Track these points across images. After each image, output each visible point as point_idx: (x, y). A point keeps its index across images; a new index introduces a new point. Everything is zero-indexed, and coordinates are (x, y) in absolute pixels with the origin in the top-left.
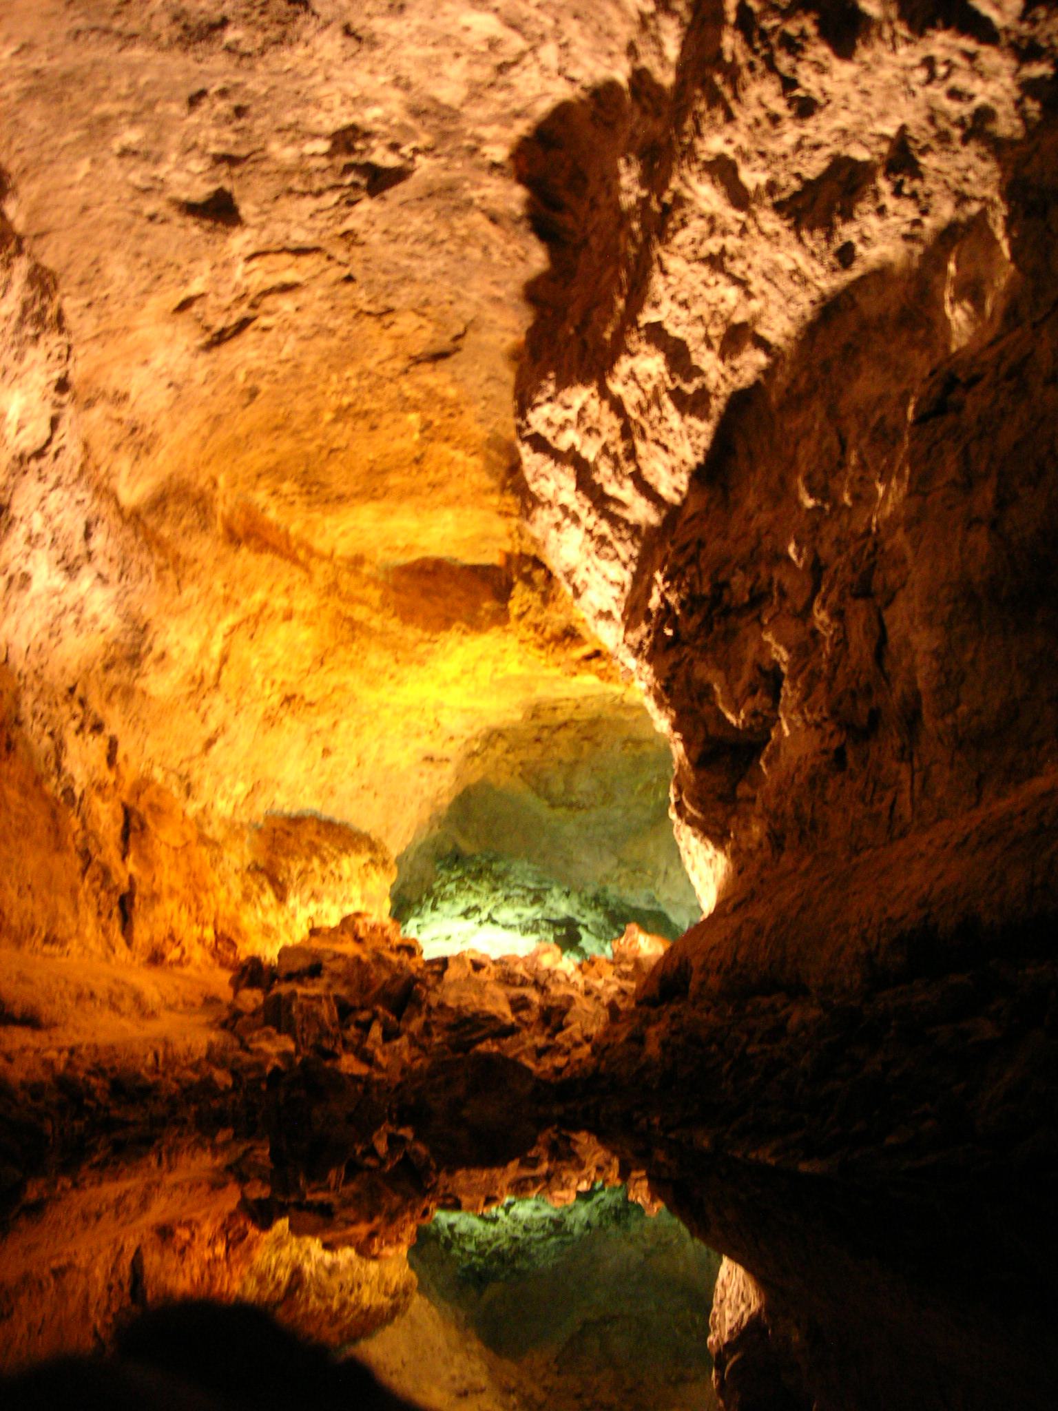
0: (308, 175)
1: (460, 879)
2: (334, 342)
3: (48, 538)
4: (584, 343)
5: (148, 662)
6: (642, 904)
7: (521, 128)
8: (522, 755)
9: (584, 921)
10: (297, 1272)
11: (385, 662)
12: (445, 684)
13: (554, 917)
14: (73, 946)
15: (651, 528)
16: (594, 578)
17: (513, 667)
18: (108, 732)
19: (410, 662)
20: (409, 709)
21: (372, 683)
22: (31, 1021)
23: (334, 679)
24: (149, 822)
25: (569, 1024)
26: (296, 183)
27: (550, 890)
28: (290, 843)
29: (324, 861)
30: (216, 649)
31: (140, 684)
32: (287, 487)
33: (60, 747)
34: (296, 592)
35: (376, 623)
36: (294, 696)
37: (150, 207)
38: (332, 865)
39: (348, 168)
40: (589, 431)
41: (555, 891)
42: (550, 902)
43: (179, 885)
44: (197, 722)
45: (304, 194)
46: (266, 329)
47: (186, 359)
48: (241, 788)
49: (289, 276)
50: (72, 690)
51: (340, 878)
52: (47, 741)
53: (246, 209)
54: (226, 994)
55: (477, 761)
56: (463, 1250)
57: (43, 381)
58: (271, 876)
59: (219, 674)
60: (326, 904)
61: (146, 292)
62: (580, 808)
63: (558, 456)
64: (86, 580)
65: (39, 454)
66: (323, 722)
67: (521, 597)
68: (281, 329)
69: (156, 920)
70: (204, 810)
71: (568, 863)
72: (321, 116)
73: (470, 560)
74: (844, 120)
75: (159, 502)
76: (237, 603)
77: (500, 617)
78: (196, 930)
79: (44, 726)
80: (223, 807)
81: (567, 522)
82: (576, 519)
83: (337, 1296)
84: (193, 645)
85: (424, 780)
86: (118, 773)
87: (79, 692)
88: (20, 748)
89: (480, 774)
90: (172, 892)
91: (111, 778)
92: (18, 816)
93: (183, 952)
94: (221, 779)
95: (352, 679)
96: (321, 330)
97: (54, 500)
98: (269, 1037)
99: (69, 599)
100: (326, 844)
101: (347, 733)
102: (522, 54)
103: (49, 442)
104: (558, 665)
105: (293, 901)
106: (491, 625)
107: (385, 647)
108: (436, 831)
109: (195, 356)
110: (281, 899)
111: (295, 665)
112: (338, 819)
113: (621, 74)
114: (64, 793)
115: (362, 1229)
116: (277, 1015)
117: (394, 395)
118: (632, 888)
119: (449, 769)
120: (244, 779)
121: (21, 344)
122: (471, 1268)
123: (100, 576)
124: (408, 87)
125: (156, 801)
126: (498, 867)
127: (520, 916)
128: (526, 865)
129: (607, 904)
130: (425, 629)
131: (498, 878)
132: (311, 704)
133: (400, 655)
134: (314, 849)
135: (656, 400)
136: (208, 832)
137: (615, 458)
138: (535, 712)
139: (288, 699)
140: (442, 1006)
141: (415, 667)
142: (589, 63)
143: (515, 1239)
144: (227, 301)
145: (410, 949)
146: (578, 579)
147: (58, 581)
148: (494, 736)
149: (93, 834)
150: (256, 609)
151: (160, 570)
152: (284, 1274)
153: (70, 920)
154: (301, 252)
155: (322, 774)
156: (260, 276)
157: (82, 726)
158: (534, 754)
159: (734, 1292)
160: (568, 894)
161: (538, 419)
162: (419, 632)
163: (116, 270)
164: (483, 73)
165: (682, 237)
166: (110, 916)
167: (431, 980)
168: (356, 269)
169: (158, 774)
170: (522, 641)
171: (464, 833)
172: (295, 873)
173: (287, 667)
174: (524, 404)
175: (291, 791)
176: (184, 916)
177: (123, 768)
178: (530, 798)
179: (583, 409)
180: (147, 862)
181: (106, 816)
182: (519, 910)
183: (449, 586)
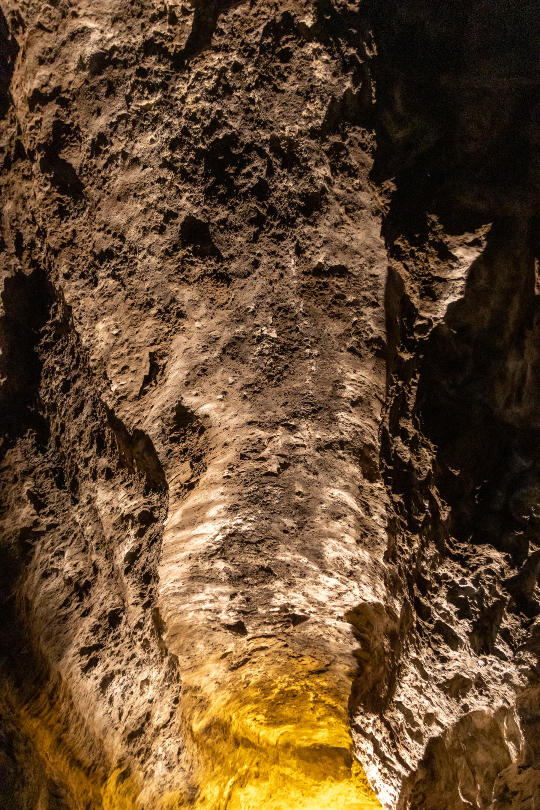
0: (271, 618)
2: (279, 666)
3: (164, 755)
4: (374, 698)
5: (197, 803)
7: (348, 608)
11: (297, 795)
15: (404, 776)
17: (354, 800)
19: (308, 795)
26: (266, 620)
30: (226, 794)
32: (261, 717)
34: (261, 765)
35: (294, 776)
37: (213, 626)
39: (285, 617)
40: (377, 730)
45: (270, 624)
46: (254, 663)
47: (224, 674)
49: (263, 645)
53: (249, 628)
57: (169, 700)
61: (210, 653)
63: (365, 735)
64: (177, 768)
65: (165, 726)
68: (260, 662)
72: (277, 601)
73: (335, 745)
74: (457, 663)
75: (208, 729)
76: (236, 771)
77: (348, 774)
81: (371, 762)
82: (374, 762)
84: (216, 792)
96: (274, 662)
97: (168, 742)
99: (168, 778)
102: (347, 591)
103: (169, 721)
106: (343, 779)
107: (298, 787)
109: (227, 672)
111: (259, 798)
113: (383, 603)
117: (303, 684)
121: (163, 689)
124: (307, 596)
130: (315, 779)
133: (304, 792)
135: (401, 729)
137: (388, 744)
141: (311, 798)
142: (372, 597)
144: (240, 654)
146: (377, 785)
147: (165, 771)
154: (268, 636)
156: (253, 645)
161: (358, 720)
163: (200, 646)
164: (333, 594)
165: (405, 678)
168: (289, 642)
170: (358, 787)
173: (256, 800)
174: (352, 713)
179: (375, 721)
183: (325, 758)
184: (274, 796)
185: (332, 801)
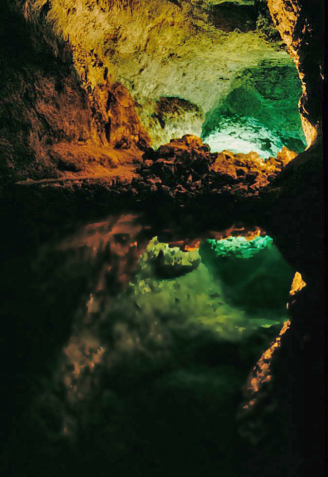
1: (229, 122)
5: (119, 42)
6: (294, 137)
8: (257, 79)
9: (272, 140)
10: (161, 252)
11: (208, 42)
12: (230, 52)
13: (262, 138)
14: (88, 141)
16: (284, 18)
17: (256, 47)
18: (104, 66)
20: (215, 60)
21: (202, 50)
22: (73, 168)
23: (189, 48)
24: (117, 99)
25: (256, 182)
27: (261, 128)
28: (168, 106)
29: (179, 114)
30: (145, 37)
31: (117, 49)
33: (87, 71)
35: (204, 28)
36: (174, 54)
38: (182, 116)
41: (263, 129)
42: (261, 132)
43: (126, 121)
44: (137, 63)
48: (152, 87)
50: (92, 51)
51: (184, 120)
52: (82, 69)
54: (141, 160)
55: (240, 80)
56: (219, 249)
58: (159, 118)
59: (146, 46)
60: (179, 130)
62: (276, 100)
66: (183, 64)
67: (260, 20)
69: (118, 133)
70: (138, 94)
71: (268, 119)
76: (154, 19)
77: (253, 27)
78: (132, 137)
79: (82, 64)
80: (145, 93)
83: (174, 261)
85: (219, 86)
86: (107, 81)
87: (95, 52)
88: (72, 72)
89: (240, 85)
90: (124, 124)
91: (105, 83)
92: (70, 97)
93: (127, 145)
94: (145, 83)
95: (196, 49)
98: (154, 178)
100: (180, 108)
101: (192, 68)
104: (273, 47)
105: (167, 128)
108: (222, 104)
110: (163, 127)
111: (174, 43)
112: (186, 99)
114: (88, 88)
115: (182, 242)
116: (157, 170)
118: (290, 130)
119: (229, 83)
120: (153, 83)
122: (222, 255)
123: (102, 9)
125: (121, 91)
126: (243, 118)
127: (250, 137)
128: (253, 119)
129: (281, 135)
130: (224, 31)
131: (243, 122)
132: (179, 57)
134: (176, 109)
136: (139, 102)
138: (263, 63)
139: (171, 55)
140: (213, 171)
141: (219, 45)
143: (237, 247)
145: (206, 148)
146: (278, 17)
148: (247, 71)
149: (97, 102)
150: (160, 21)
151: (124, 6)
152: (157, 253)
153: (87, 133)
155: (182, 82)
157: (95, 64)
158: (260, 79)
159: (298, 283)
160: (267, 130)
162: (222, 31)
166: (102, 132)
167: (211, 161)
169: (122, 81)
171: (232, 105)
172: (168, 118)
173: (171, 44)
175: (171, 88)
176: (128, 132)
177: (109, 79)
178: (258, 95)
180: (116, 113)
181: (102, 96)
182: (249, 134)
184: (187, 42)
185: (237, 48)
